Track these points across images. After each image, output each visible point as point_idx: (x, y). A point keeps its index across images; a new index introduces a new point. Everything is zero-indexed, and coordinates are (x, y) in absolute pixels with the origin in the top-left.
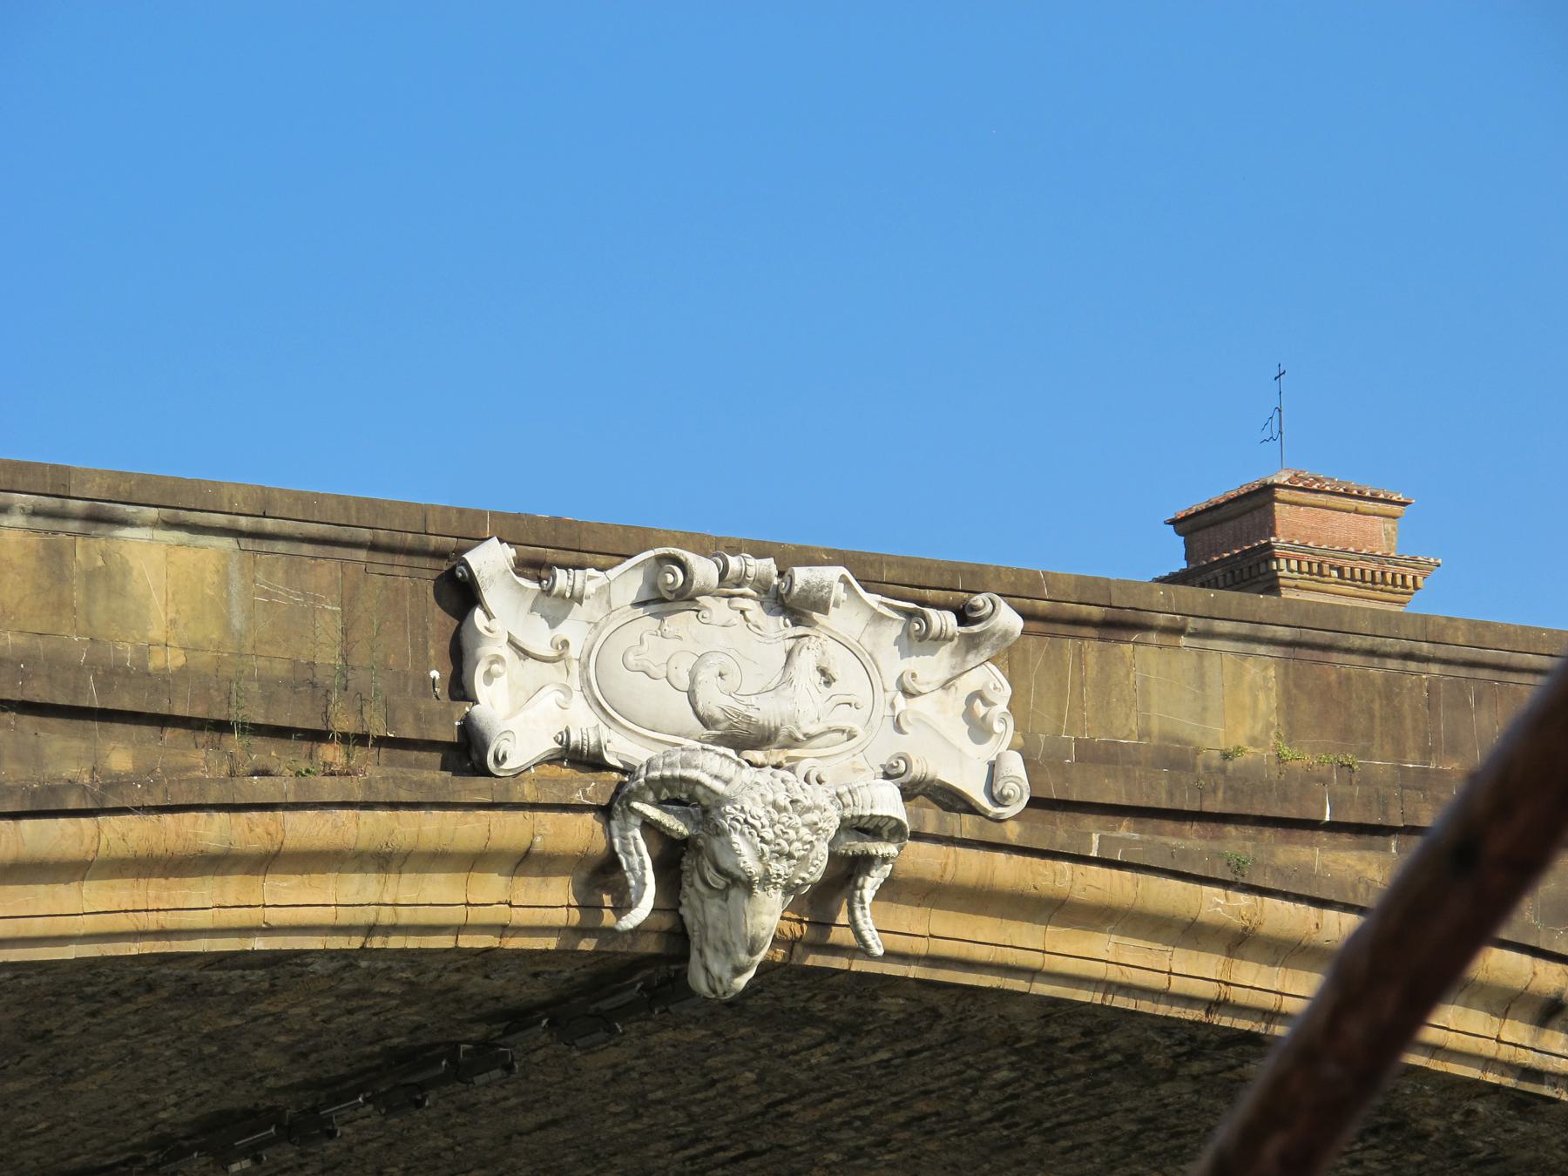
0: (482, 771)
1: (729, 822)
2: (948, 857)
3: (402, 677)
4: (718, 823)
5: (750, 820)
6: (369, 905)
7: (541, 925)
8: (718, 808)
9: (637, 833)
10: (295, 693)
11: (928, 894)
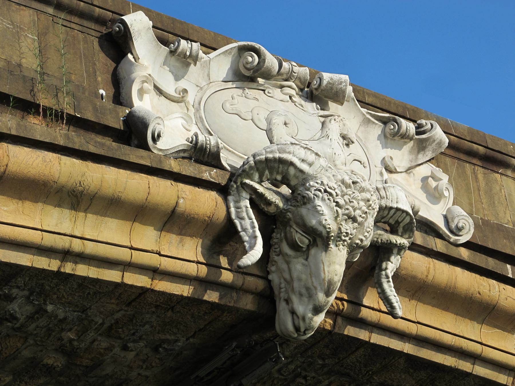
0: (144, 146)
1: (313, 192)
2: (430, 264)
3: (81, 89)
4: (305, 195)
5: (328, 190)
6: (65, 235)
7: (180, 272)
8: (304, 185)
9: (247, 203)
10: (11, 75)
11: (416, 292)
